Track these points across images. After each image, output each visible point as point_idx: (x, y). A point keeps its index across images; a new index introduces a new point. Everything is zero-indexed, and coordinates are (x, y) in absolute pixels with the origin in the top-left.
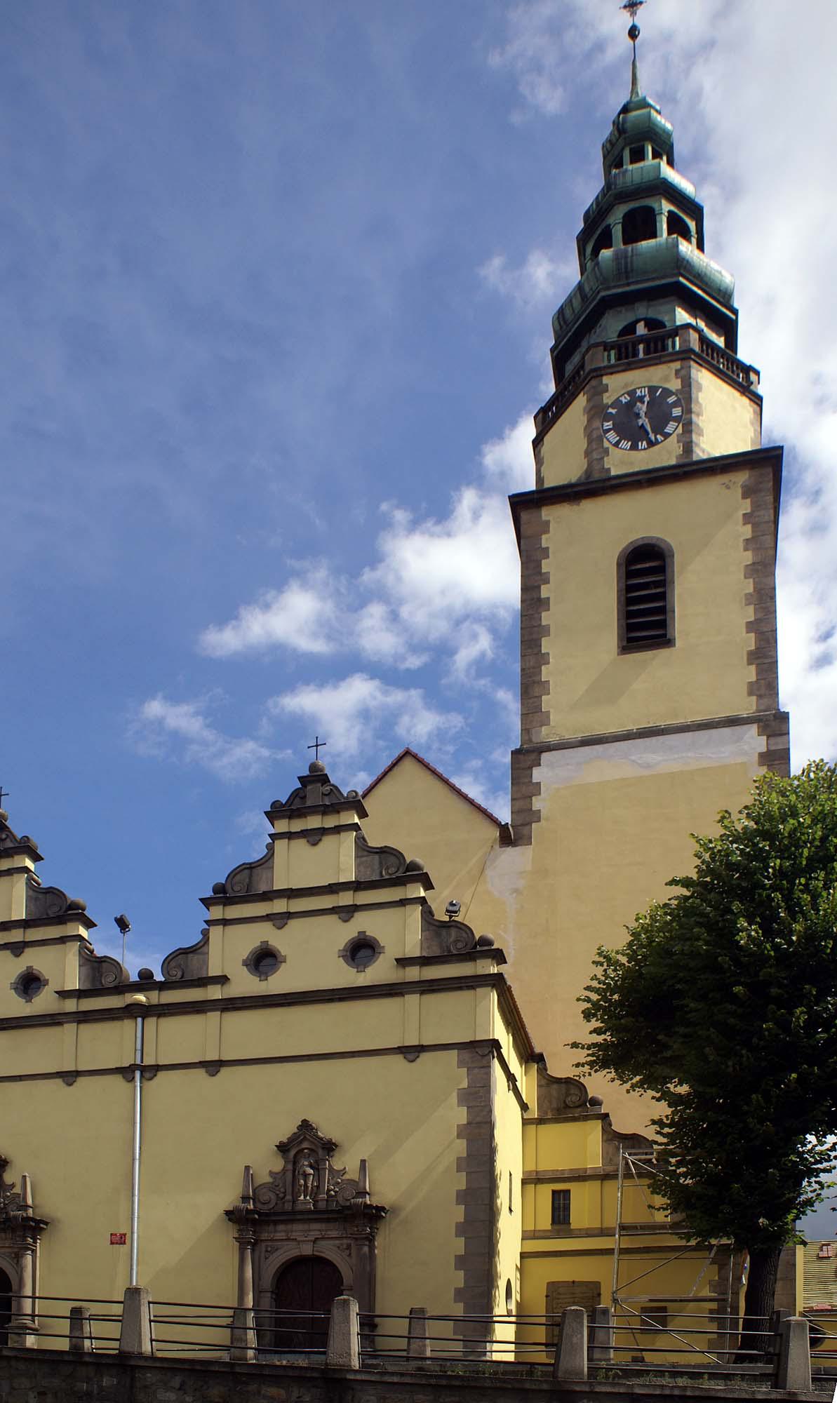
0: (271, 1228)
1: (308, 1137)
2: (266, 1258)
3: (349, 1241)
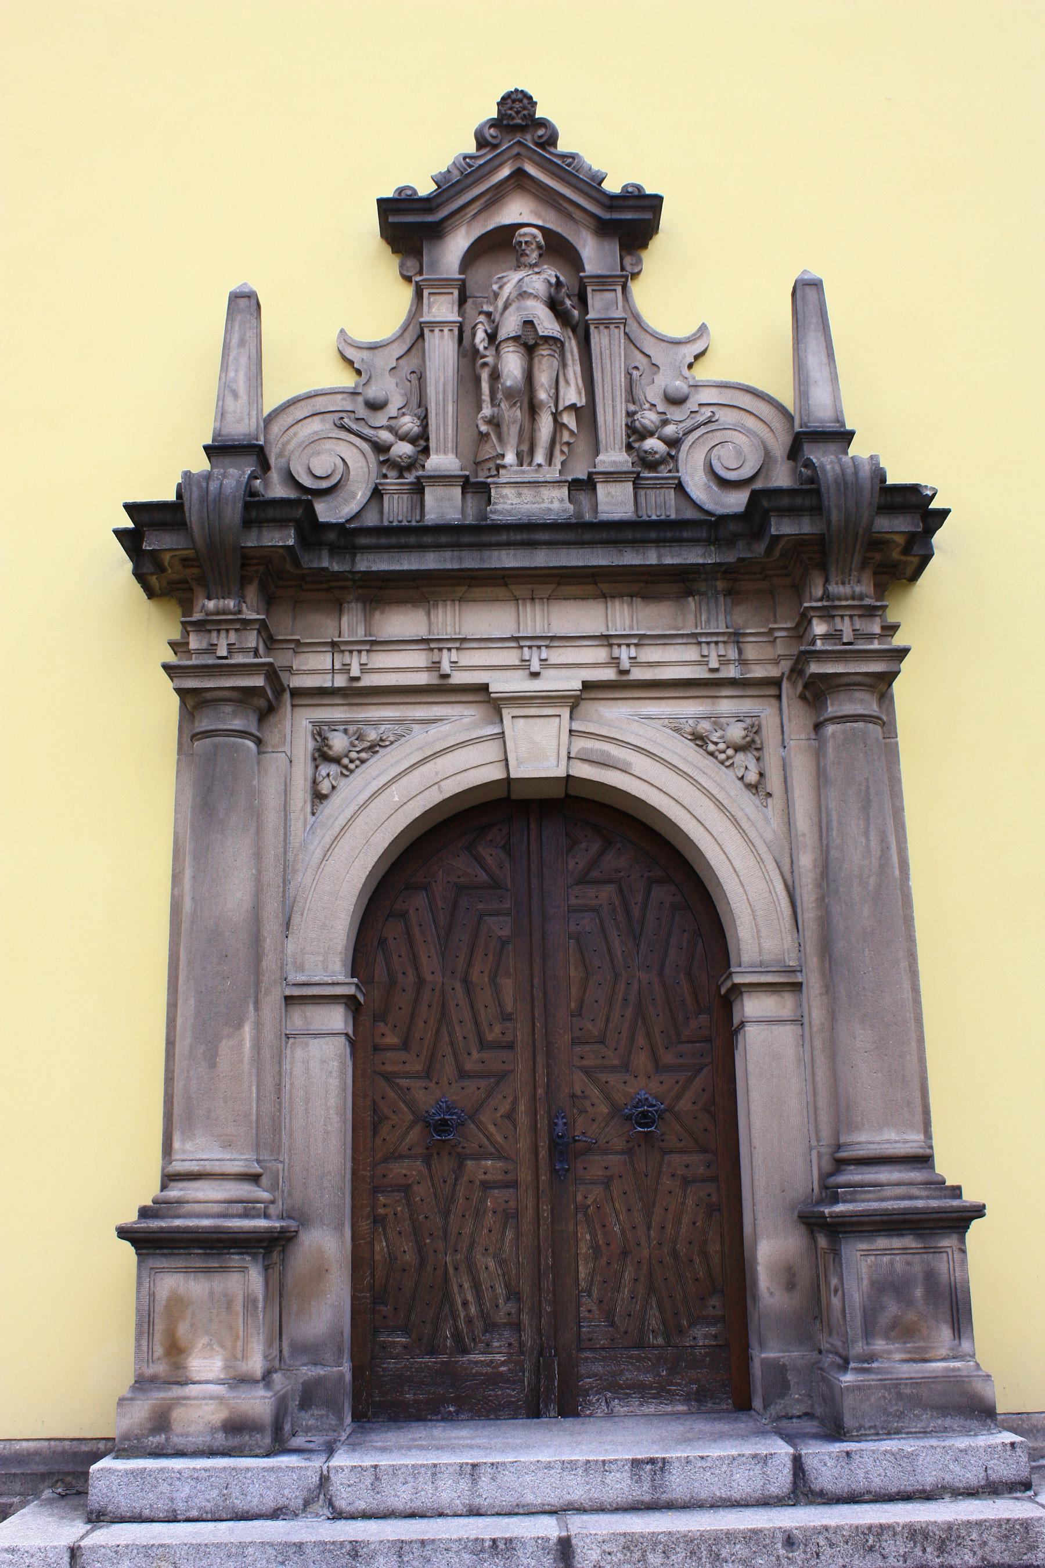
1: (531, 169)
2: (319, 797)
3: (747, 706)
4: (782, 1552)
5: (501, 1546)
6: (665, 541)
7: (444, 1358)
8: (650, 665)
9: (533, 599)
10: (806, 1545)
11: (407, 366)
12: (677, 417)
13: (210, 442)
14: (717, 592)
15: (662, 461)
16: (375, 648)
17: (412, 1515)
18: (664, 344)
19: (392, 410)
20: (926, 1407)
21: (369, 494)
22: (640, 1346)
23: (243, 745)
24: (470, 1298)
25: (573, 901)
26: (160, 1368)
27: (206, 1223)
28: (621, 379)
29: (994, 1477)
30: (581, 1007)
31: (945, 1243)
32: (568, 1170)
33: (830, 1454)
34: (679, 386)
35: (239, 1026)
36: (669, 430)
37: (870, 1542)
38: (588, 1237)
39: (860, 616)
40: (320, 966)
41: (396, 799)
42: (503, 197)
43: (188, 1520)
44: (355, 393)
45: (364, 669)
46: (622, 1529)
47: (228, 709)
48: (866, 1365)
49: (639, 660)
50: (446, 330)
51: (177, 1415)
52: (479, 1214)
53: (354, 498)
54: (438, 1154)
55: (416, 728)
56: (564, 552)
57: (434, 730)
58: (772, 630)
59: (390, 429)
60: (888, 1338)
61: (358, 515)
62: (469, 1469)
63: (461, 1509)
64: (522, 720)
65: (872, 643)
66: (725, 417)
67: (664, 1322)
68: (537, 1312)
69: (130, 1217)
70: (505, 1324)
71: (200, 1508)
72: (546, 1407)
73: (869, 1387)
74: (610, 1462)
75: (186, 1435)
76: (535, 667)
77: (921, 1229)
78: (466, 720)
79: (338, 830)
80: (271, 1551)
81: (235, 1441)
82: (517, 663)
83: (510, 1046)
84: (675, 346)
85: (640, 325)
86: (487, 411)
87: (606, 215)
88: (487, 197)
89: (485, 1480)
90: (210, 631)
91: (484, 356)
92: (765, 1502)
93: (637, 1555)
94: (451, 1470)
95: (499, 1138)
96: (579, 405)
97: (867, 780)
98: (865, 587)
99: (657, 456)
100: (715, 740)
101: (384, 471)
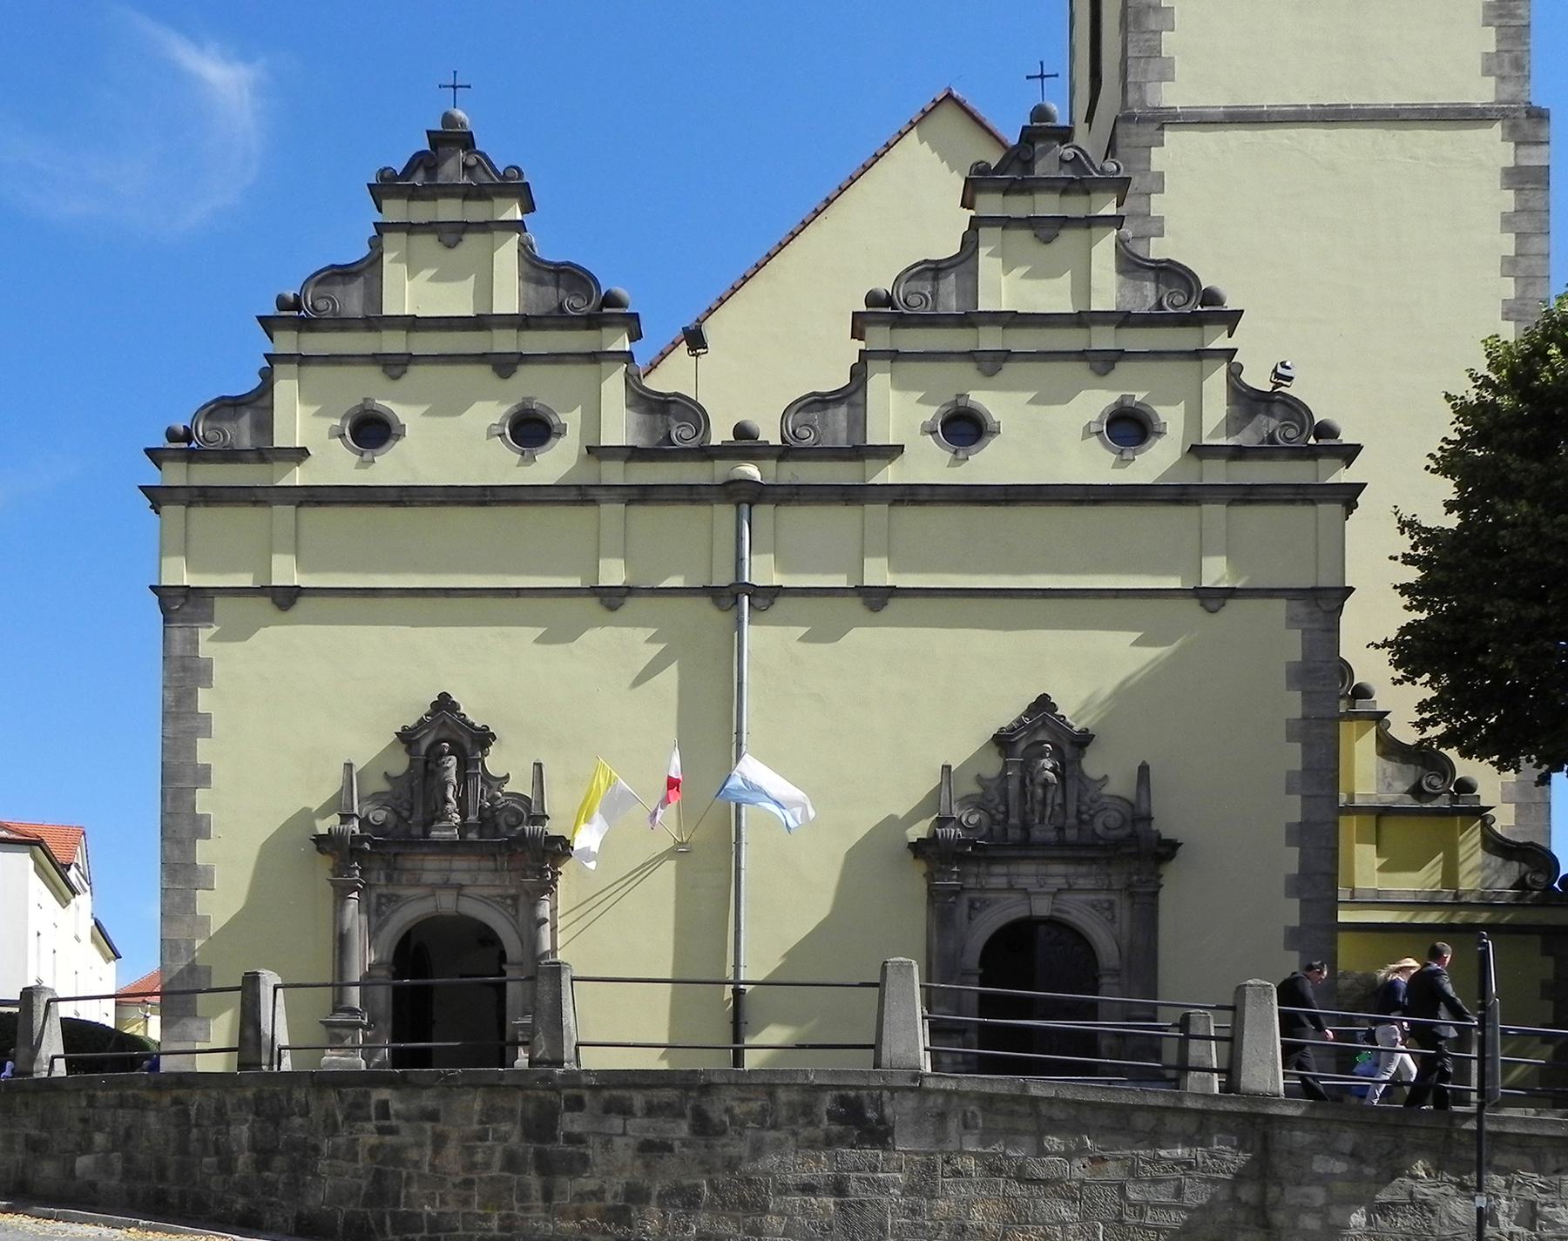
28: (1076, 794)
36: (1091, 812)
86: (1029, 805)
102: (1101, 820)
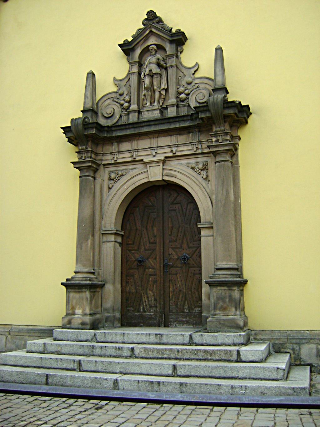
0: (114, 148)
1: (154, 30)
3: (205, 159)
4: (176, 353)
5: (120, 348)
6: (180, 121)
7: (140, 313)
8: (180, 151)
9: (154, 138)
10: (181, 352)
11: (128, 84)
12: (189, 88)
13: (82, 110)
14: (196, 132)
15: (185, 100)
16: (119, 153)
17: (112, 343)
18: (187, 69)
19: (125, 95)
20: (226, 326)
21: (119, 116)
22: (183, 312)
23: (89, 178)
24: (146, 300)
25: (170, 209)
26: (70, 312)
27: (78, 282)
29: (235, 342)
30: (171, 234)
31: (234, 289)
32: (167, 272)
33: (198, 335)
34: (190, 80)
35: (87, 240)
36: (186, 92)
37: (195, 353)
38: (172, 287)
39: (224, 135)
40: (109, 226)
41: (126, 188)
42: (149, 38)
43: (71, 341)
44: (117, 92)
45: (117, 158)
46: (144, 347)
47: (85, 171)
48: (214, 316)
49: (178, 150)
50: (135, 74)
51: (72, 321)
52: (148, 281)
53: (116, 118)
54: (140, 268)
55: (130, 170)
56: (157, 126)
57: (134, 171)
58: (208, 140)
59: (124, 100)
60: (220, 310)
61: (117, 122)
62: (122, 334)
63: (121, 342)
64: (152, 167)
65: (227, 142)
66: (202, 86)
67: (188, 307)
68: (160, 304)
69: (65, 281)
70: (154, 306)
71: (73, 339)
72: (161, 325)
73: (213, 321)
74: (151, 334)
75: (74, 325)
76: (154, 154)
77: (228, 285)
78: (141, 168)
79: (113, 196)
80: (78, 346)
81: (83, 327)
82: (150, 154)
83: (155, 243)
84: (189, 69)
85: (181, 65)
87: (171, 39)
88: (144, 39)
89: (126, 336)
90: (81, 154)
91: (143, 80)
92: (183, 344)
93: (147, 352)
94: (119, 334)
95: (153, 264)
96: (165, 88)
97: (224, 177)
98: (227, 127)
99: (183, 99)
100: (196, 168)
101: (123, 110)
102: (194, 97)
